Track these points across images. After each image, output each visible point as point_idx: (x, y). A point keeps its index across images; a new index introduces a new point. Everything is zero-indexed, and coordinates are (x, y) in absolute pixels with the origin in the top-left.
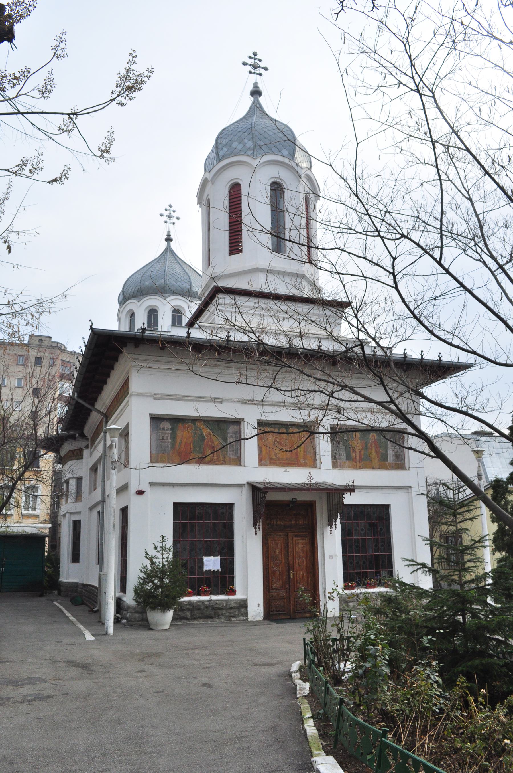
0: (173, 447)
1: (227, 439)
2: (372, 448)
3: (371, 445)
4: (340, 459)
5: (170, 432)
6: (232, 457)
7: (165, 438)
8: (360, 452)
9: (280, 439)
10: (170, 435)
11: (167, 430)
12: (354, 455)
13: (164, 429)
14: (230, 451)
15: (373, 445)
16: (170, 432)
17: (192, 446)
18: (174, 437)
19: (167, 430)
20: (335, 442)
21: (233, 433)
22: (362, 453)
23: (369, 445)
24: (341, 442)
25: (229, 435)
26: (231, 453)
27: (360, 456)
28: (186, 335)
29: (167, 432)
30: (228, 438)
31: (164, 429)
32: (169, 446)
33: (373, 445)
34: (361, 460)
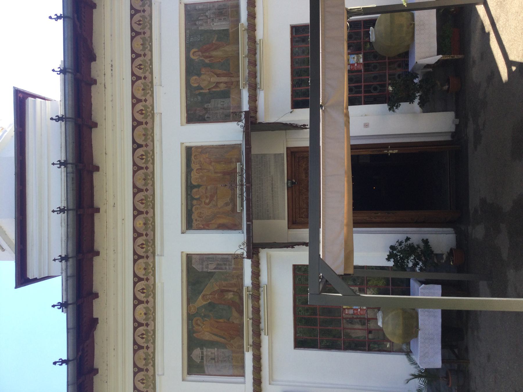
0: (224, 346)
1: (210, 273)
2: (210, 57)
3: (207, 57)
4: (229, 108)
5: (205, 349)
6: (233, 266)
7: (213, 356)
8: (218, 75)
9: (207, 197)
10: (209, 350)
11: (202, 353)
12: (222, 87)
13: (202, 358)
14: (226, 269)
15: (207, 54)
16: (205, 349)
17: (221, 320)
18: (212, 344)
19: (202, 353)
20: (206, 116)
21: (203, 265)
22: (219, 71)
23: (207, 61)
24: (206, 106)
25: (205, 270)
26: (227, 267)
27: (225, 75)
28: (65, 366)
29: (205, 353)
30: (209, 271)
31: (202, 358)
32: (222, 350)
33: (207, 54)
34: (228, 75)
